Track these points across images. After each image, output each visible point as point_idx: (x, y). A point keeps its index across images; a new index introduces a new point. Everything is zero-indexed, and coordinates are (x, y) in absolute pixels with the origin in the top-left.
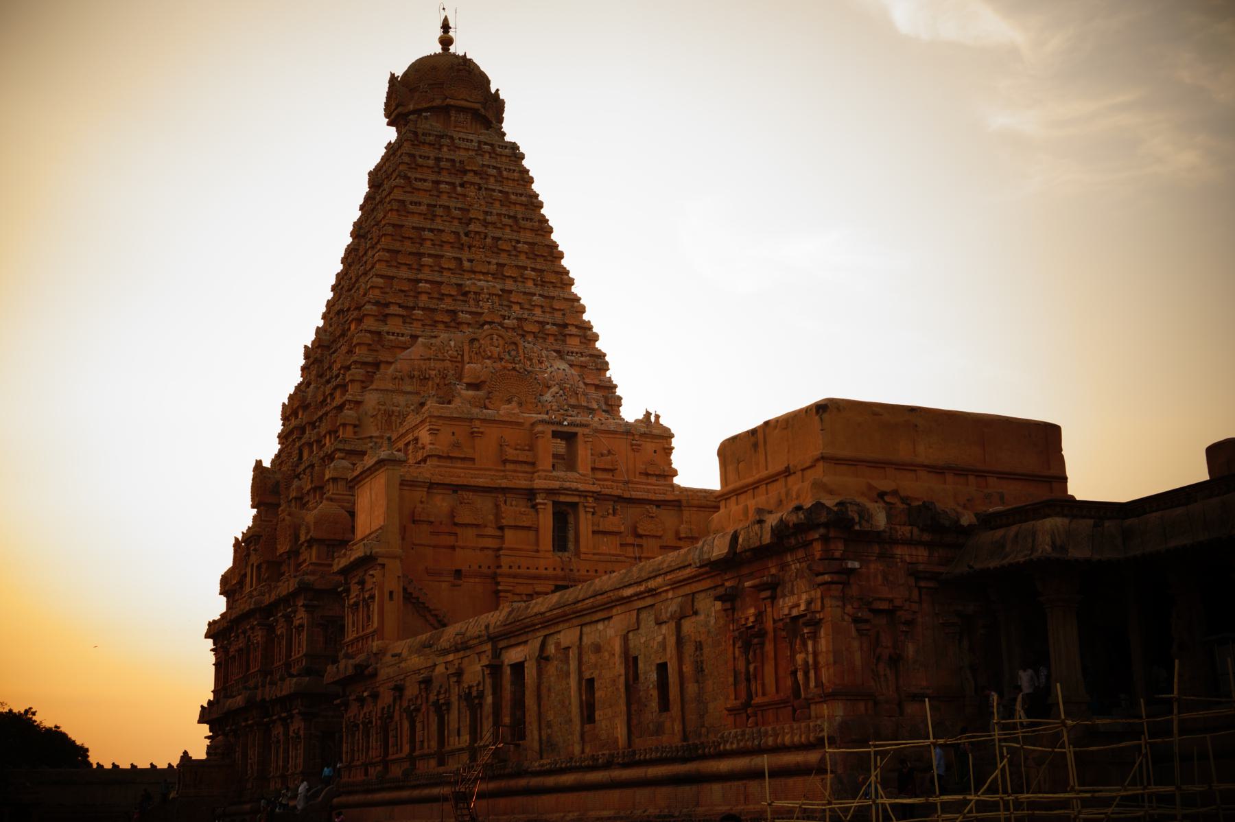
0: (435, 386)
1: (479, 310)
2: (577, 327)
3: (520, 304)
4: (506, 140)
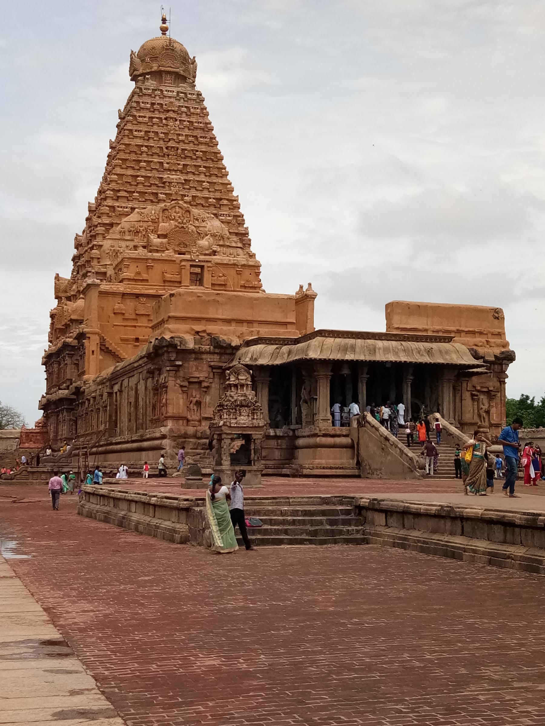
0: (143, 236)
1: (170, 192)
2: (227, 200)
3: (195, 188)
4: (196, 90)
